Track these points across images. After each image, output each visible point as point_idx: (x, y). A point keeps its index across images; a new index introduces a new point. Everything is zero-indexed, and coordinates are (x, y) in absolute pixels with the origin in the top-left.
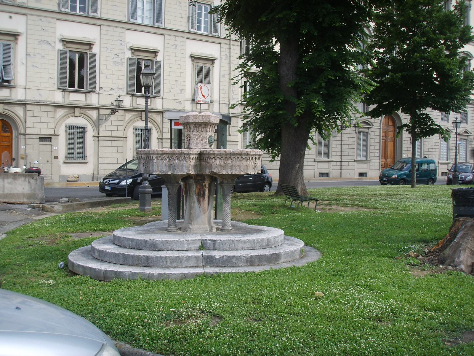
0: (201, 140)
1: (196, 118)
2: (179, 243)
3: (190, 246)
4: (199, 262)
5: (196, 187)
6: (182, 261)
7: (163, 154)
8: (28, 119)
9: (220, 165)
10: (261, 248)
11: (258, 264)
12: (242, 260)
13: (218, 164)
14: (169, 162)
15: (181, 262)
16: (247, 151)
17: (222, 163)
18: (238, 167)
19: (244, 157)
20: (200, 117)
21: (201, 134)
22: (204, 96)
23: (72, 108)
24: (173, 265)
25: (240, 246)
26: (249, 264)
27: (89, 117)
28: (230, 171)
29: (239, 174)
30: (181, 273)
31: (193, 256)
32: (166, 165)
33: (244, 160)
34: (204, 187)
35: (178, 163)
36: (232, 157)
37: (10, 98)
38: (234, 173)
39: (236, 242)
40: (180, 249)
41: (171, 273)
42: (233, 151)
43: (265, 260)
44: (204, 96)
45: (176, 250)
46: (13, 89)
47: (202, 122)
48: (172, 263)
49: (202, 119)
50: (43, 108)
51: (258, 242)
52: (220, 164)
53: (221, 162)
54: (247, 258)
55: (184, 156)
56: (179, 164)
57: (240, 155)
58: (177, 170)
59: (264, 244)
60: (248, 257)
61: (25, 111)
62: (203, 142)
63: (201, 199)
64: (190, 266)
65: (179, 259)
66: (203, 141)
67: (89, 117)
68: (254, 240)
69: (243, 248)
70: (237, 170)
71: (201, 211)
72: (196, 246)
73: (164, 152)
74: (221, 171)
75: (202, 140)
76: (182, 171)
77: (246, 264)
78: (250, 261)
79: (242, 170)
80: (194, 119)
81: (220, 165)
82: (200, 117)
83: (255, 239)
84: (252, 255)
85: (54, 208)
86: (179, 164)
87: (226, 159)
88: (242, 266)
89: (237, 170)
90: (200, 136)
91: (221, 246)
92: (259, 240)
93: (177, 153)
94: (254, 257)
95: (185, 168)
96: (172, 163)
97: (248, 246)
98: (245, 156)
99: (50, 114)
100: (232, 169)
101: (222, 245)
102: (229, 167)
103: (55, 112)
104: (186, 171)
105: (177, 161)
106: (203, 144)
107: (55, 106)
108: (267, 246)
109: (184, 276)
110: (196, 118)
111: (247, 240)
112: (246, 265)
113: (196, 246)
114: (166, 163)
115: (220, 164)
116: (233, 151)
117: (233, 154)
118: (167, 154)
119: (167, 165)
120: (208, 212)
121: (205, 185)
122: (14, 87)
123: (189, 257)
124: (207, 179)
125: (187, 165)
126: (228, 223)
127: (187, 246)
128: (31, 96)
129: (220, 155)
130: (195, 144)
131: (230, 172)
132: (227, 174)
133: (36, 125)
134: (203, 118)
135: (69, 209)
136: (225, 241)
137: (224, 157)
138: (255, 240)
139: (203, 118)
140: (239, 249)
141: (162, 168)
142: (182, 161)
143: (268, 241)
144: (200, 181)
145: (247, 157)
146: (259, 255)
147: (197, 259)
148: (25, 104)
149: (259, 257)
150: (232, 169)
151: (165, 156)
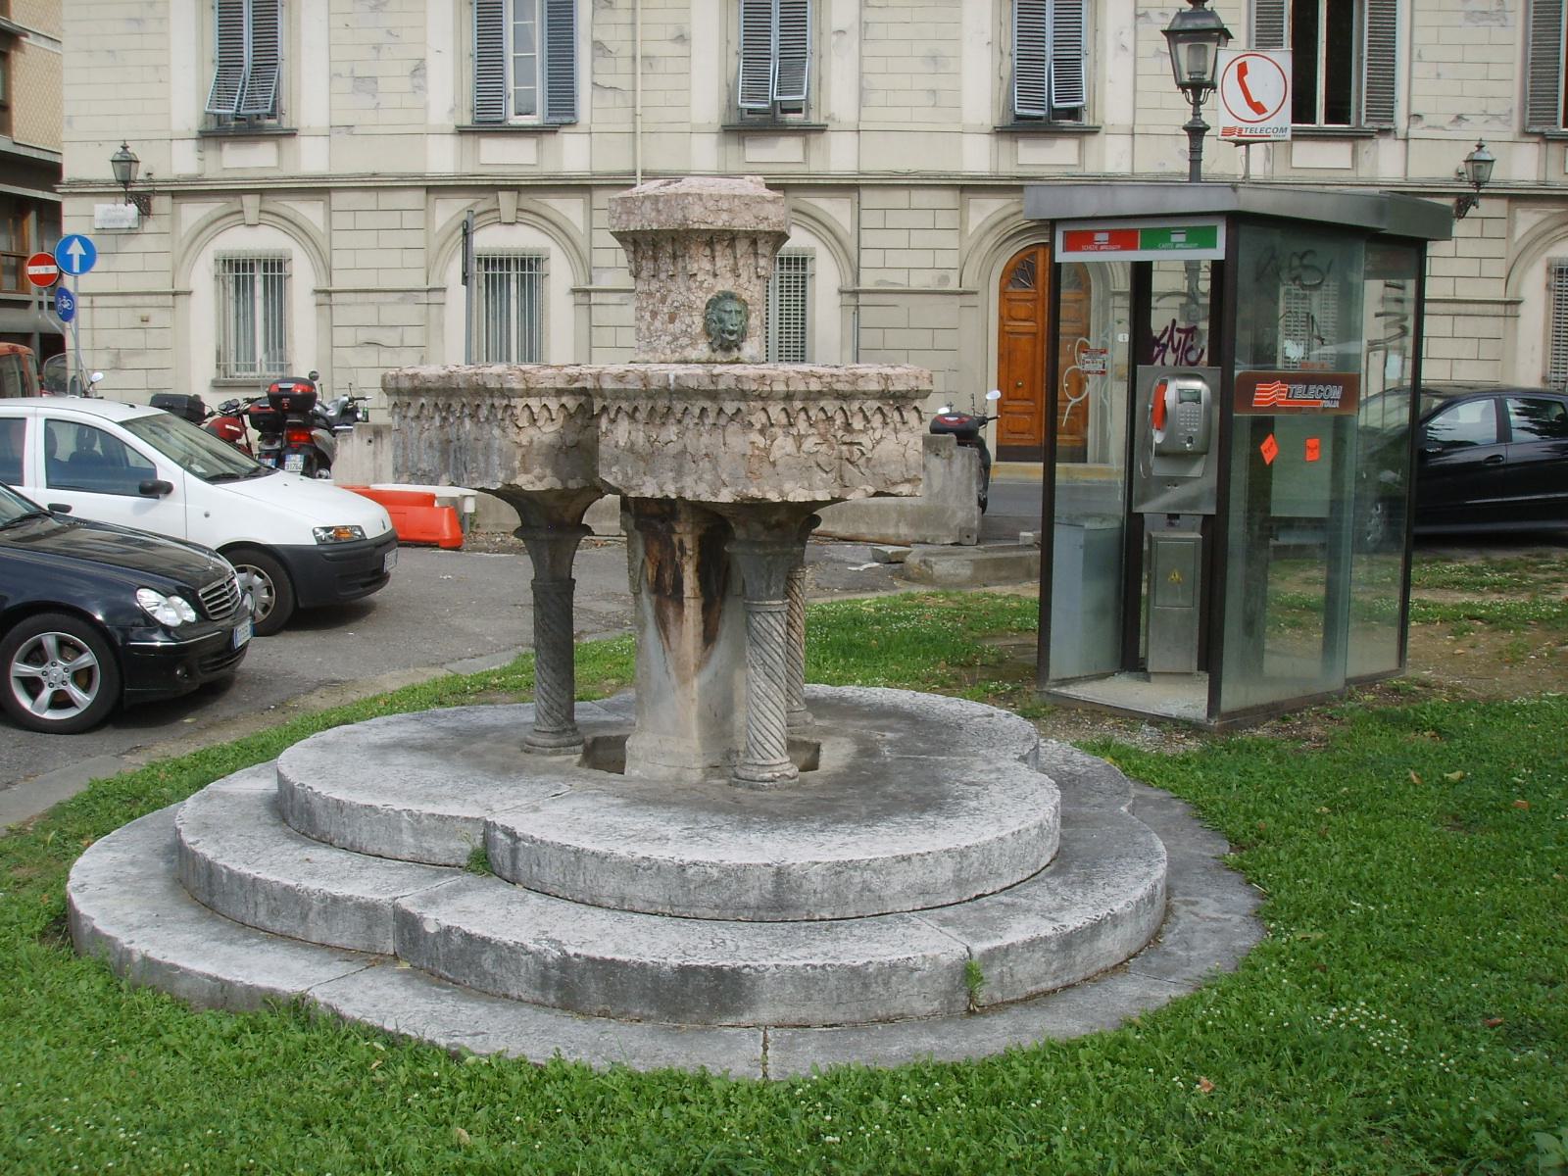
0: (666, 317)
1: (630, 212)
2: (379, 821)
3: (425, 845)
4: (379, 931)
5: (647, 553)
6: (307, 915)
7: (415, 392)
8: (868, 239)
9: (631, 449)
10: (729, 913)
11: (601, 1007)
12: (523, 970)
13: (622, 443)
14: (442, 427)
15: (304, 917)
16: (738, 378)
17: (640, 438)
18: (705, 464)
19: (730, 407)
20: (648, 204)
21: (670, 291)
22: (1258, 108)
23: (511, 190)
24: (277, 927)
25: (609, 886)
26: (552, 999)
27: (556, 228)
28: (675, 480)
29: (713, 499)
30: (209, 977)
31: (350, 898)
32: (431, 445)
33: (734, 427)
34: (678, 553)
35: (472, 437)
36: (678, 407)
38: (689, 495)
39: (591, 864)
40: (386, 850)
41: (178, 968)
42: (677, 377)
43: (643, 996)
44: (1258, 108)
45: (370, 850)
47: (655, 227)
48: (274, 913)
49: (654, 214)
50: (921, 198)
51: (708, 882)
52: (633, 444)
53: (633, 433)
54: (546, 965)
55: (489, 402)
56: (476, 439)
57: (713, 396)
58: (469, 468)
59: (752, 898)
60: (549, 959)
61: (330, 212)
62: (677, 326)
63: (671, 612)
64: (337, 942)
65: (296, 903)
66: (677, 323)
67: (556, 228)
68: (682, 868)
69: (623, 900)
70: (700, 478)
71: (671, 669)
72: (453, 845)
73: (416, 383)
74: (634, 482)
75: (672, 319)
76: (487, 474)
77: (537, 995)
78: (561, 985)
79: (724, 476)
80: (624, 217)
81: (631, 449)
82: (648, 204)
83: (687, 859)
84: (571, 951)
85: (931, 568)
86: (476, 439)
87: (659, 416)
88: (520, 1000)
89: (700, 478)
90: (663, 300)
91: (535, 869)
92: (715, 873)
93: (462, 385)
94: (575, 963)
95: (496, 460)
96: (452, 432)
97: (652, 896)
98: (736, 404)
99: (410, 219)
100: (679, 473)
101: (539, 865)
102: (670, 463)
103: (961, 209)
104: (501, 476)
105: (468, 423)
106: (676, 339)
107: (963, 188)
108: (772, 909)
109: (219, 995)
110: (630, 212)
111: (646, 864)
112: (541, 999)
113: (453, 845)
114: (433, 432)
115: (633, 444)
116: (677, 377)
117: (677, 391)
118: (428, 390)
119: (436, 442)
120: (707, 675)
121: (681, 542)
123: (335, 900)
124: (683, 516)
125: (505, 443)
126: (758, 746)
127: (411, 840)
129: (627, 398)
130: (644, 338)
131: (673, 488)
132: (659, 495)
133: (893, 259)
134: (661, 206)
135: (1003, 574)
136: (548, 850)
137: (644, 405)
138: (690, 871)
139: (661, 206)
140: (604, 900)
141: (419, 456)
142: (487, 427)
143: (778, 884)
144: (653, 521)
145: (743, 406)
146: (603, 961)
147: (368, 918)
149: (607, 969)
150: (679, 473)
151: (423, 400)
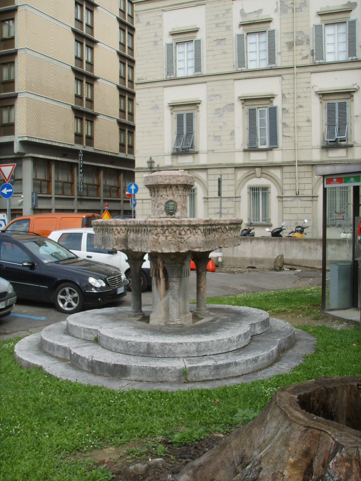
10: (137, 354)
18: (145, 243)
20: (151, 178)
31: (62, 346)
33: (150, 234)
37: (267, 161)
39: (110, 340)
46: (195, 155)
51: (133, 346)
59: (142, 350)
62: (159, 209)
68: (127, 342)
81: (133, 240)
92: (134, 344)
102: (139, 243)
108: (146, 354)
122: (197, 153)
128: (215, 160)
138: (129, 343)
148: (207, 169)
149: (100, 363)
